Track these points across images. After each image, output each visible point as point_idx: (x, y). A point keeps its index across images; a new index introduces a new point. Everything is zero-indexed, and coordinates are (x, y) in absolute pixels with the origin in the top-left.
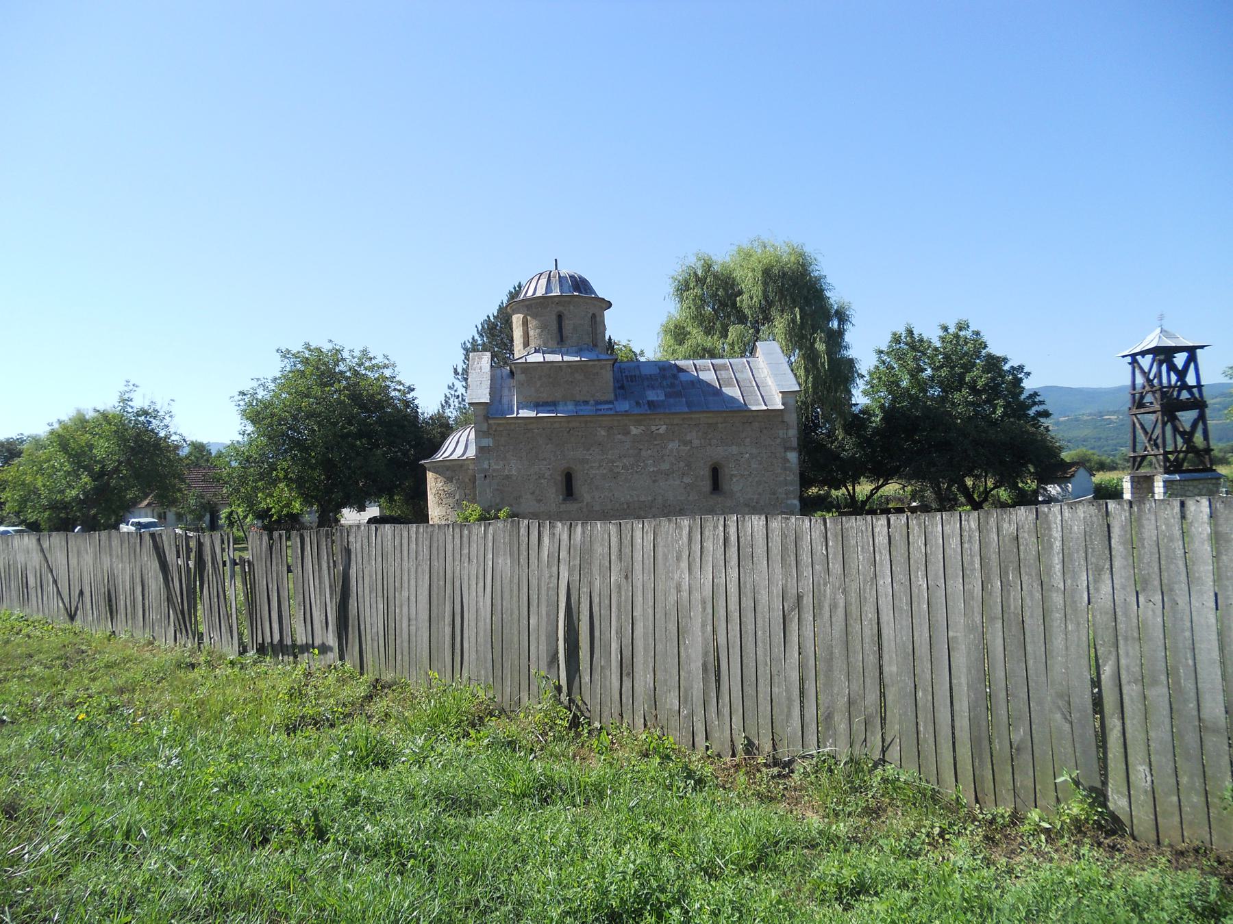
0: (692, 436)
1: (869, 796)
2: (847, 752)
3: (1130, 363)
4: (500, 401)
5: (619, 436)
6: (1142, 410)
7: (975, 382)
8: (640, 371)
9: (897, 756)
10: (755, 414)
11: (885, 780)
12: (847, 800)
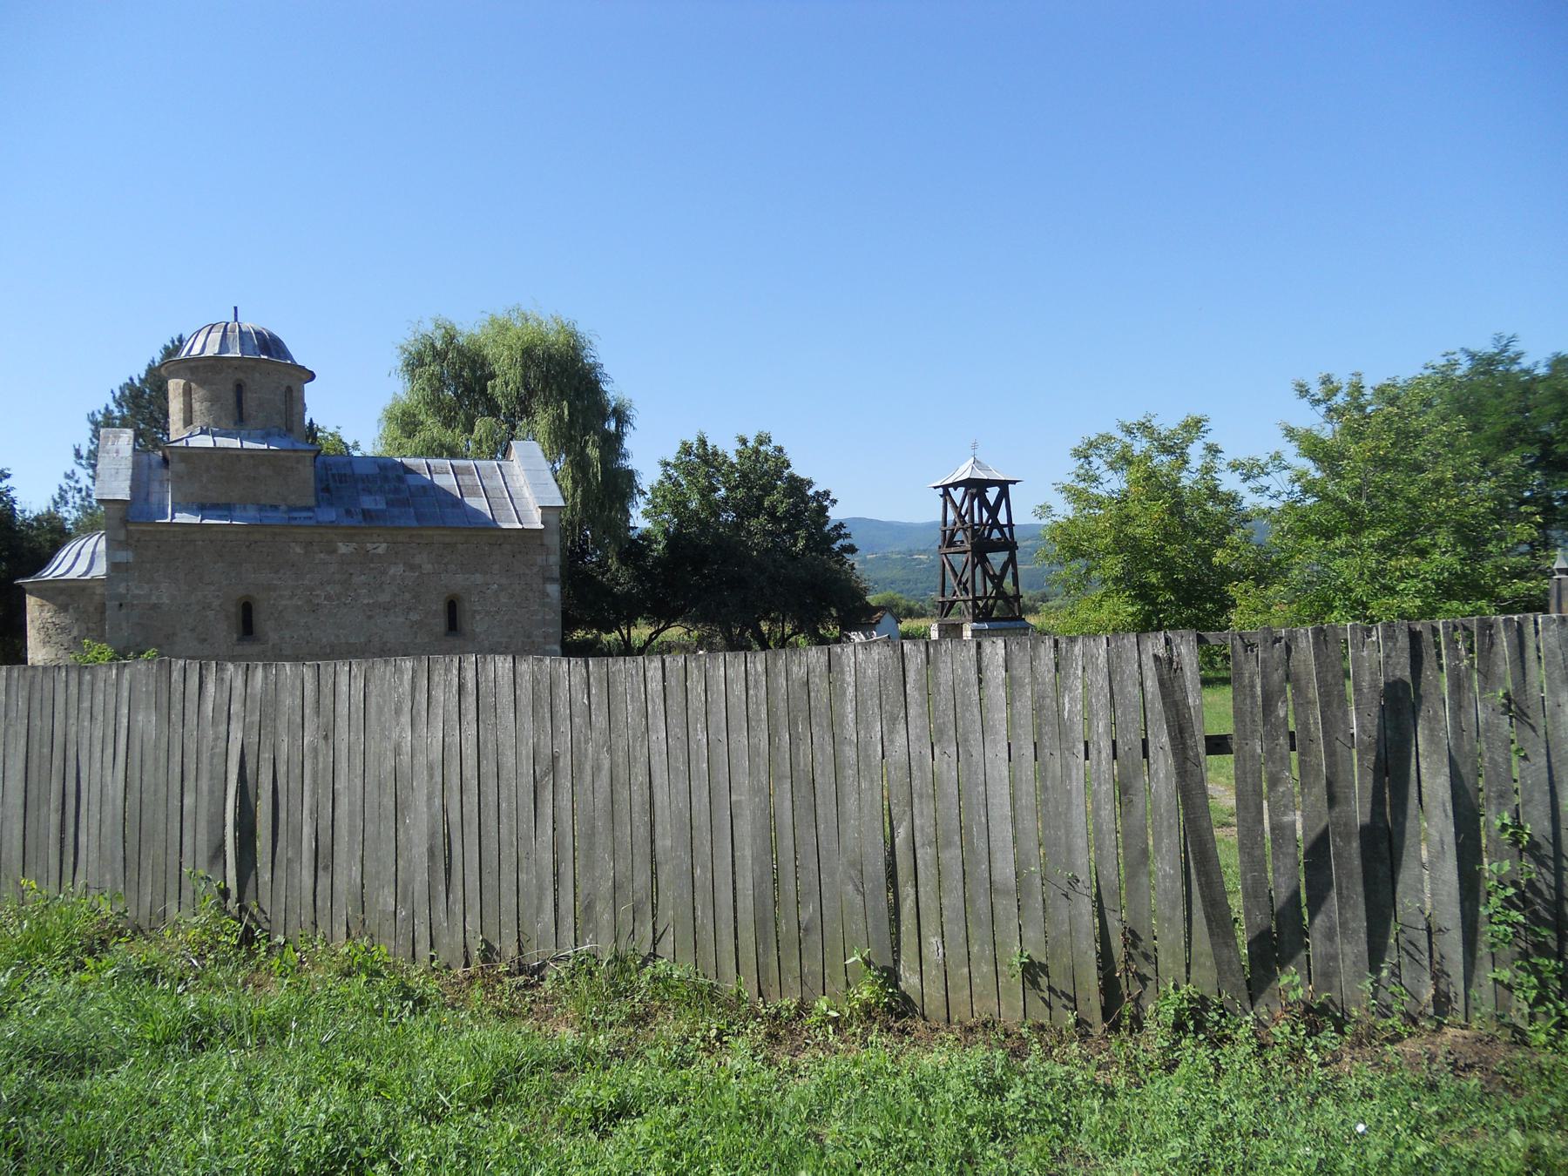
0: (424, 560)
1: (636, 1000)
2: (611, 948)
3: (941, 496)
4: (147, 499)
5: (322, 555)
6: (952, 550)
7: (774, 507)
8: (352, 469)
9: (670, 949)
10: (506, 533)
11: (655, 979)
12: (609, 1007)
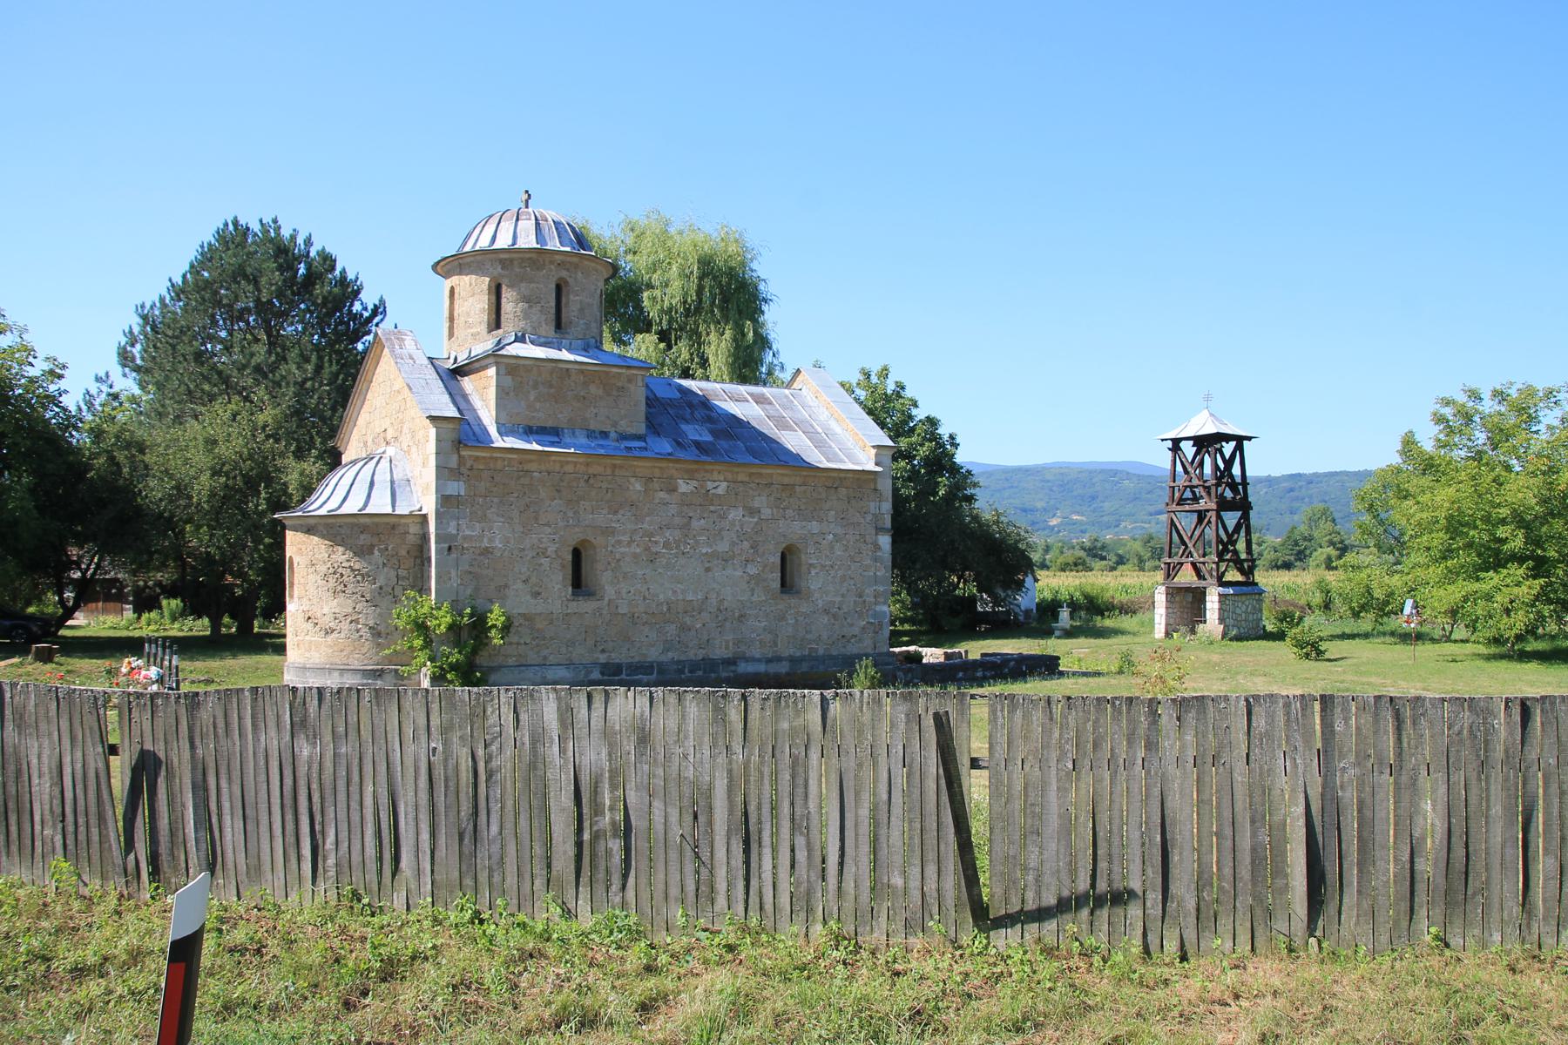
0: (760, 501)
3: (1169, 449)
5: (662, 495)
10: (842, 475)
